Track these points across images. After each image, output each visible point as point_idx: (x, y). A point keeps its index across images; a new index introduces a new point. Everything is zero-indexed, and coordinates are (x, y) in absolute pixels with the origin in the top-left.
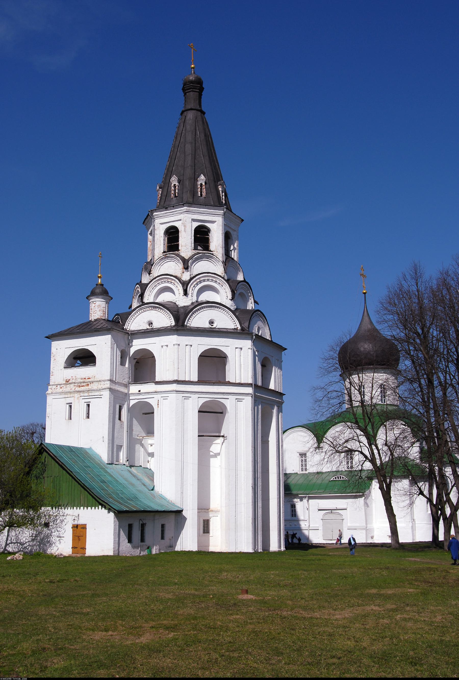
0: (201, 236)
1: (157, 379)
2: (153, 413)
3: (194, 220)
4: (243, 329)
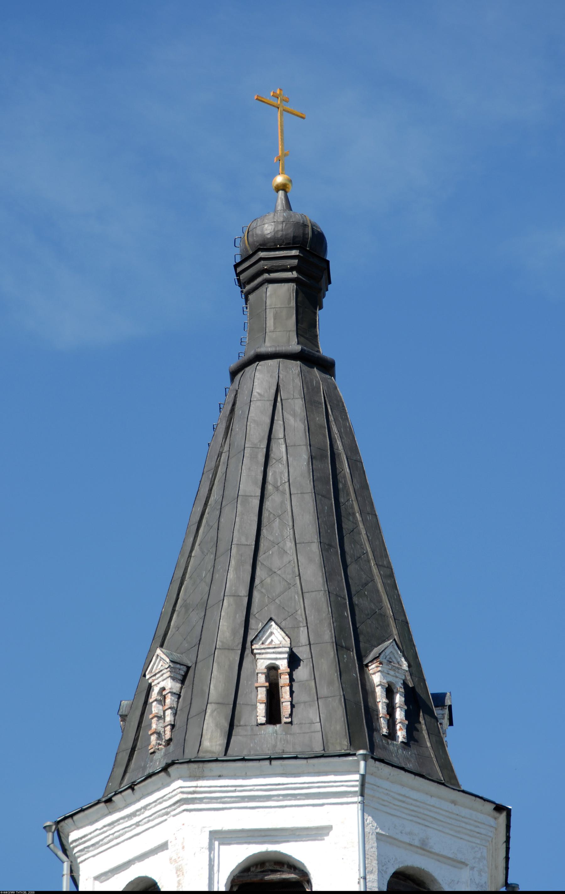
3: (220, 837)
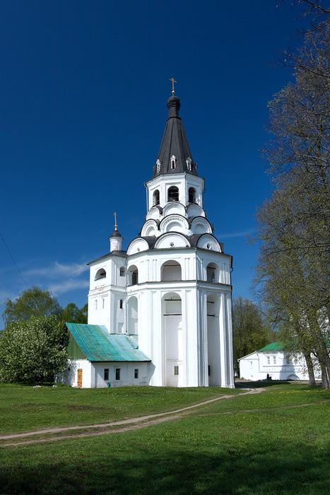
0: (191, 193)
1: (139, 282)
3: (166, 184)
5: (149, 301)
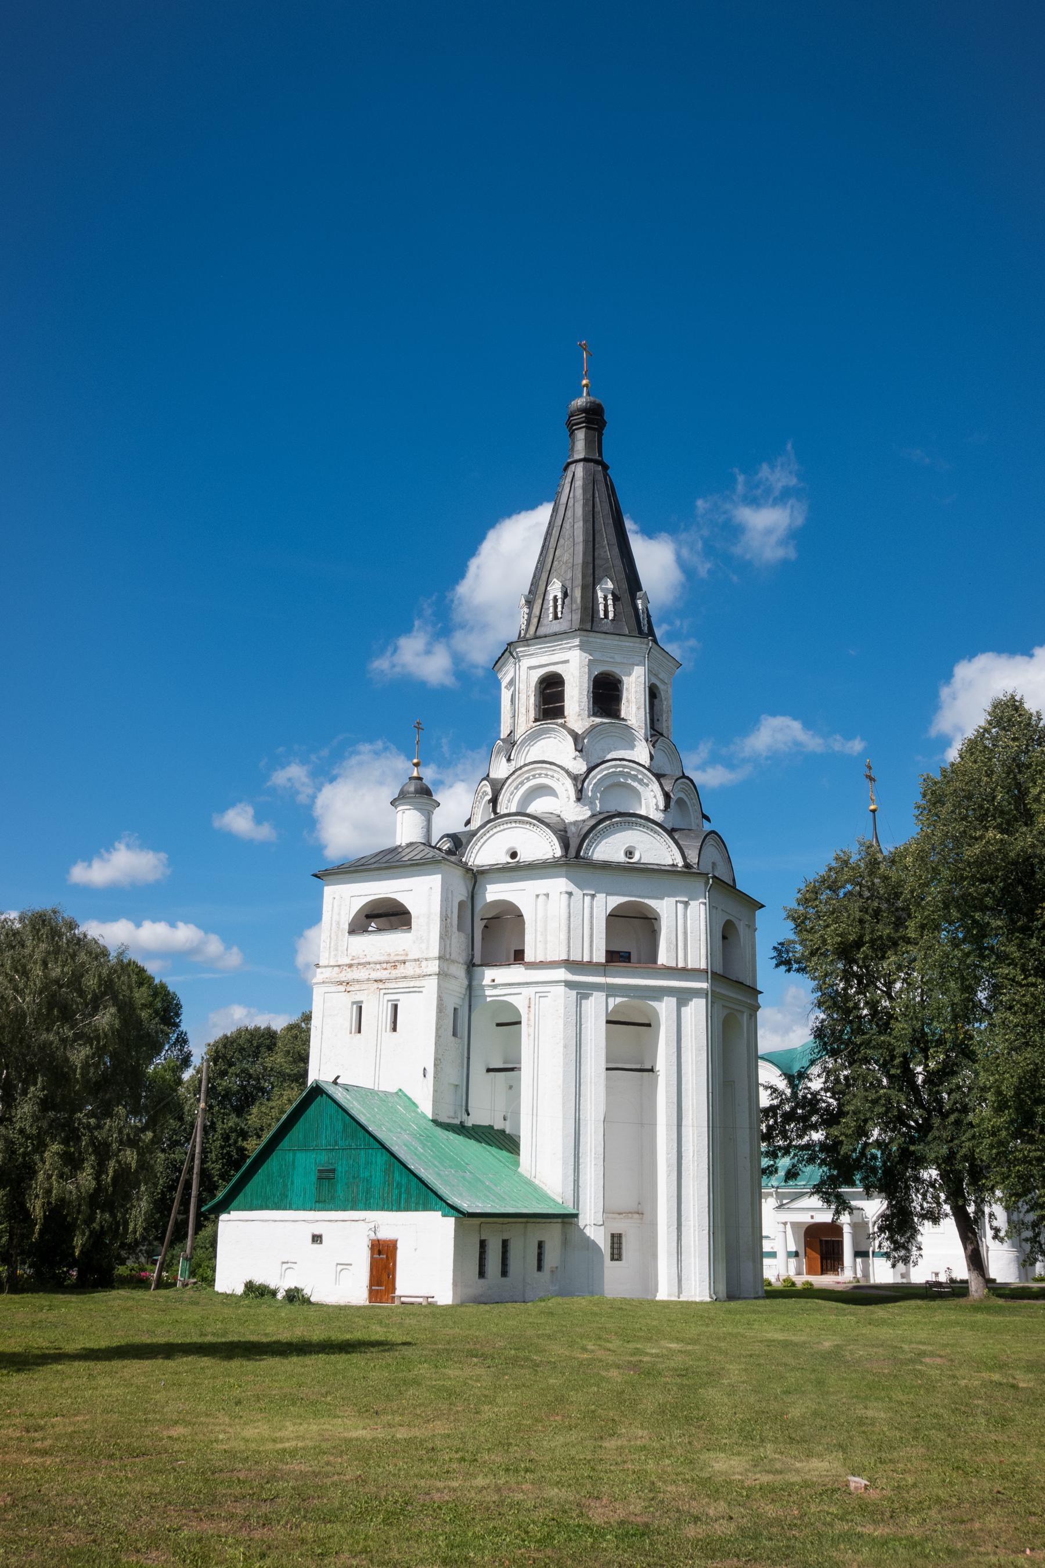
1: (529, 957)
2: (519, 1023)
4: (687, 865)
5: (552, 1020)
